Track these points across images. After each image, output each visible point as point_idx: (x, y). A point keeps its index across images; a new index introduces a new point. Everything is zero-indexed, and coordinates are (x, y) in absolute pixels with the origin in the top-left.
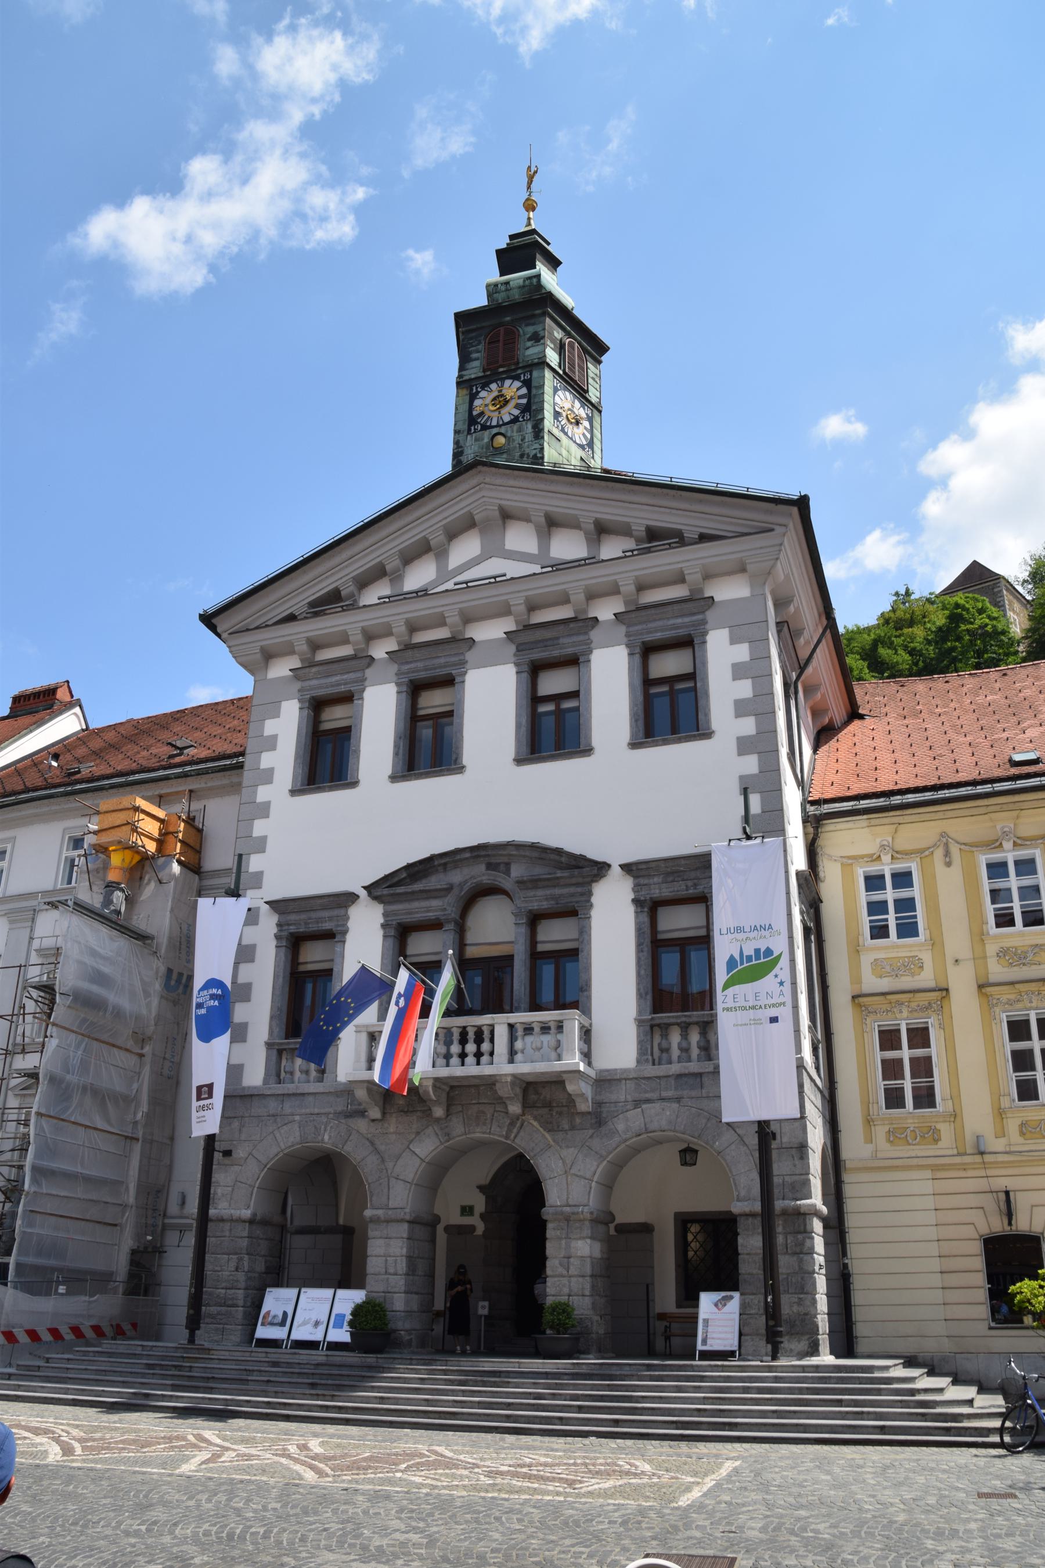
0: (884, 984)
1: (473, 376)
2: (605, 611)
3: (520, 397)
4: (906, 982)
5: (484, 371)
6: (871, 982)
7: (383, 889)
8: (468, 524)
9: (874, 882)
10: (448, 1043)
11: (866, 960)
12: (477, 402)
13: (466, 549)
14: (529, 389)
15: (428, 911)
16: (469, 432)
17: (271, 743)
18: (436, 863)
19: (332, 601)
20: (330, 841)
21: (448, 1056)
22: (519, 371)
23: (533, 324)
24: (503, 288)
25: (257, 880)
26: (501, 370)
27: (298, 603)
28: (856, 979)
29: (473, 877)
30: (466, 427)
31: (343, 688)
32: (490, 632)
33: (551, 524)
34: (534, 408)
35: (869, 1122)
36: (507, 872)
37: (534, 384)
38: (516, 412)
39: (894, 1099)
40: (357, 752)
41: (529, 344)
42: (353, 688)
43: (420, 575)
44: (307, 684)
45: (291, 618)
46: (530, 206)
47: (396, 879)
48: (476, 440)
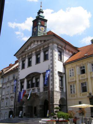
0: (71, 81)
2: (41, 49)
4: (73, 81)
6: (70, 81)
7: (28, 77)
9: (70, 71)
11: (69, 79)
13: (32, 45)
19: (23, 52)
20: (23, 74)
25: (19, 78)
27: (20, 53)
28: (68, 80)
32: (34, 52)
33: (38, 41)
35: (69, 95)
39: (71, 93)
43: (29, 48)
45: (20, 54)
46: (41, 6)
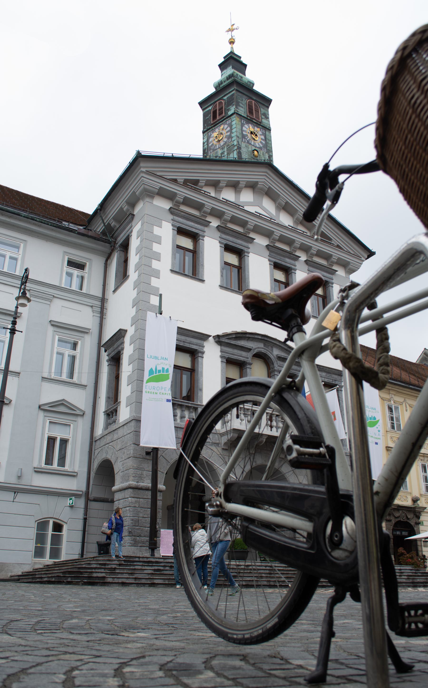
1: (243, 115)
3: (262, 139)
5: (247, 116)
8: (252, 186)
10: (271, 421)
12: (244, 128)
14: (265, 137)
15: (241, 356)
16: (242, 141)
17: (158, 240)
18: (247, 336)
21: (271, 427)
22: (261, 127)
23: (264, 109)
24: (240, 78)
26: (254, 121)
27: (181, 178)
29: (259, 348)
30: (240, 136)
31: (194, 230)
34: (268, 148)
36: (272, 350)
37: (267, 137)
38: (261, 146)
40: (203, 265)
41: (263, 117)
42: (200, 233)
44: (176, 218)
46: (232, 42)
47: (230, 337)
48: (246, 146)
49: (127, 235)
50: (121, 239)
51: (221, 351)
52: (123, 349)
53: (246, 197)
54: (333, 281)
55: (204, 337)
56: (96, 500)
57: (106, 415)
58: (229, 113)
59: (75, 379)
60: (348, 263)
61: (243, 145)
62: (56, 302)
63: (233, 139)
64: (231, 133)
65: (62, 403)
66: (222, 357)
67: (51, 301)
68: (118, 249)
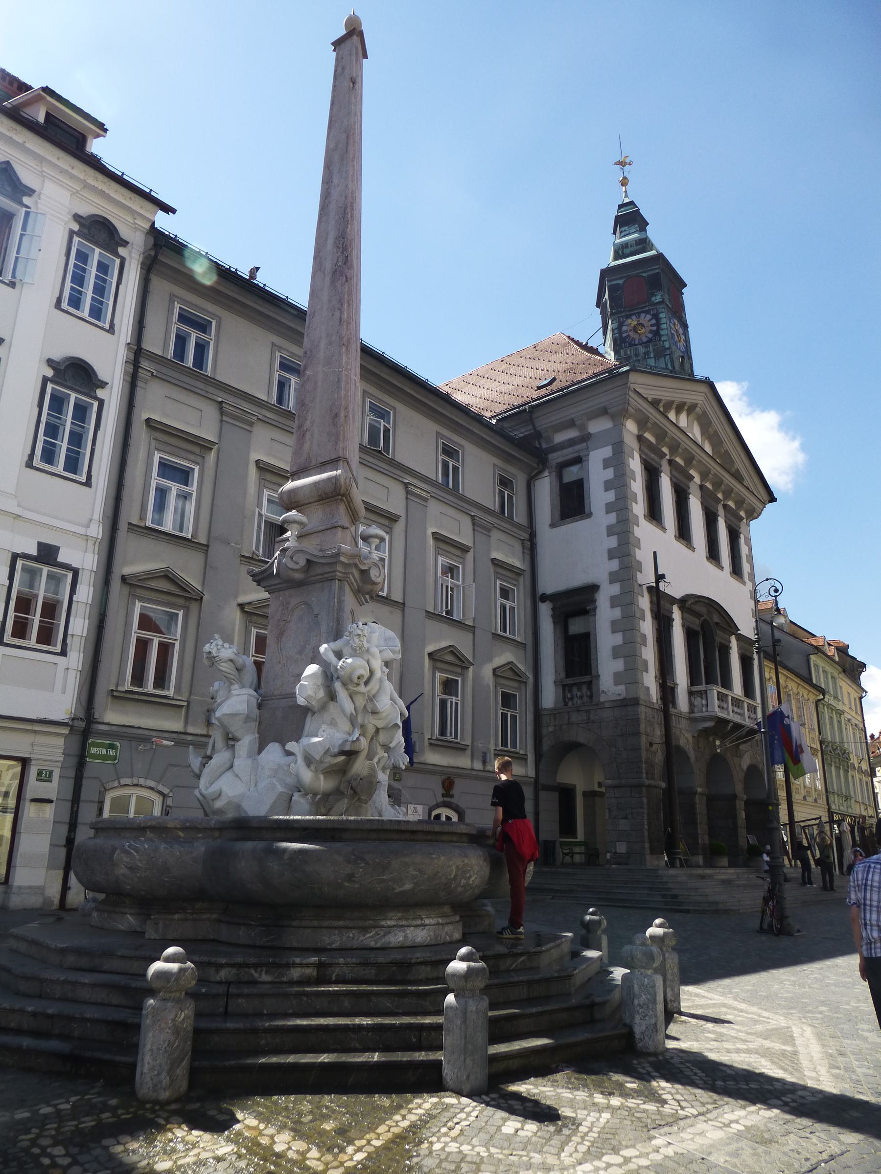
27: (651, 394)
46: (624, 182)
49: (576, 455)
50: (556, 458)
51: (683, 618)
52: (595, 609)
53: (683, 421)
54: (742, 530)
55: (672, 600)
56: (547, 788)
57: (560, 688)
58: (653, 299)
59: (516, 638)
60: (754, 510)
61: (674, 347)
62: (496, 535)
63: (663, 338)
64: (659, 328)
65: (510, 666)
66: (683, 626)
67: (489, 530)
68: (554, 469)
